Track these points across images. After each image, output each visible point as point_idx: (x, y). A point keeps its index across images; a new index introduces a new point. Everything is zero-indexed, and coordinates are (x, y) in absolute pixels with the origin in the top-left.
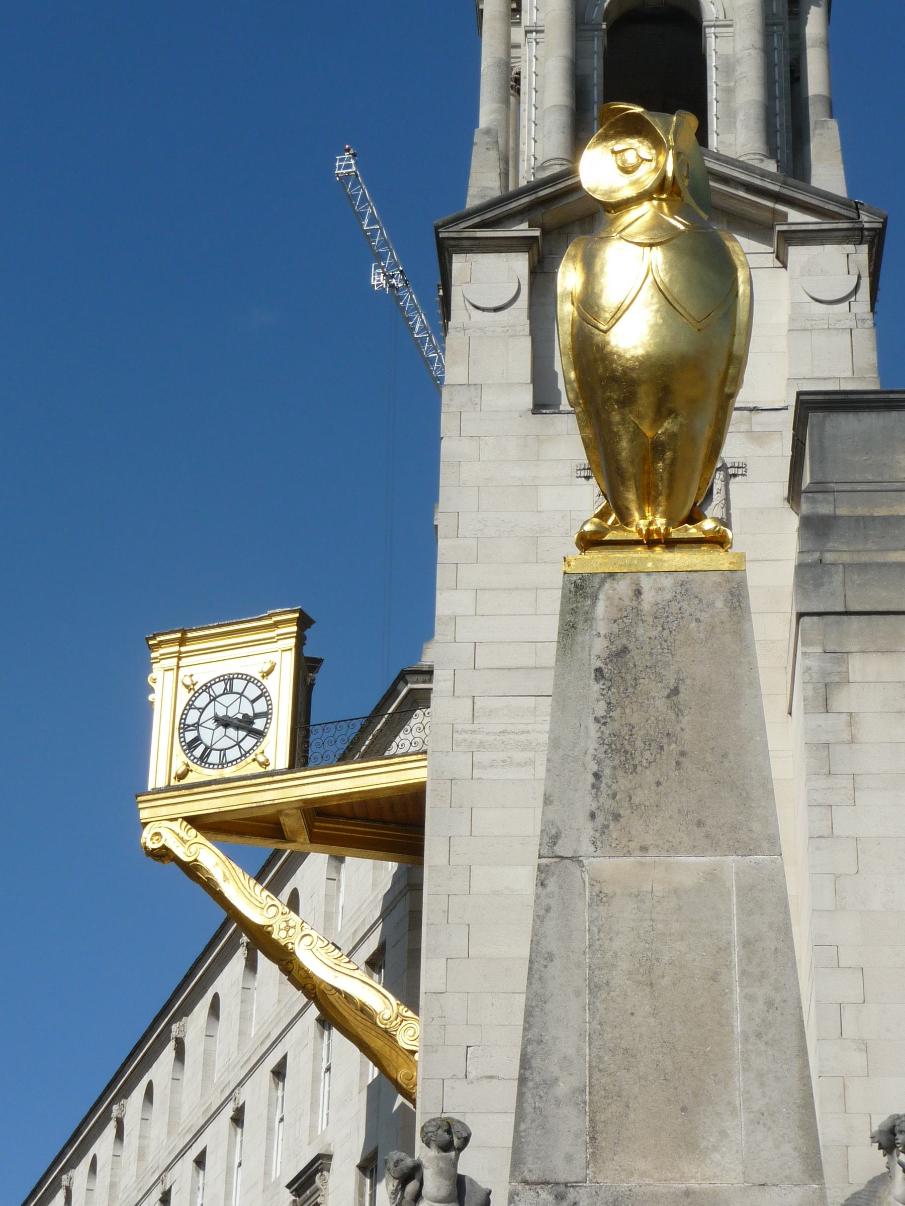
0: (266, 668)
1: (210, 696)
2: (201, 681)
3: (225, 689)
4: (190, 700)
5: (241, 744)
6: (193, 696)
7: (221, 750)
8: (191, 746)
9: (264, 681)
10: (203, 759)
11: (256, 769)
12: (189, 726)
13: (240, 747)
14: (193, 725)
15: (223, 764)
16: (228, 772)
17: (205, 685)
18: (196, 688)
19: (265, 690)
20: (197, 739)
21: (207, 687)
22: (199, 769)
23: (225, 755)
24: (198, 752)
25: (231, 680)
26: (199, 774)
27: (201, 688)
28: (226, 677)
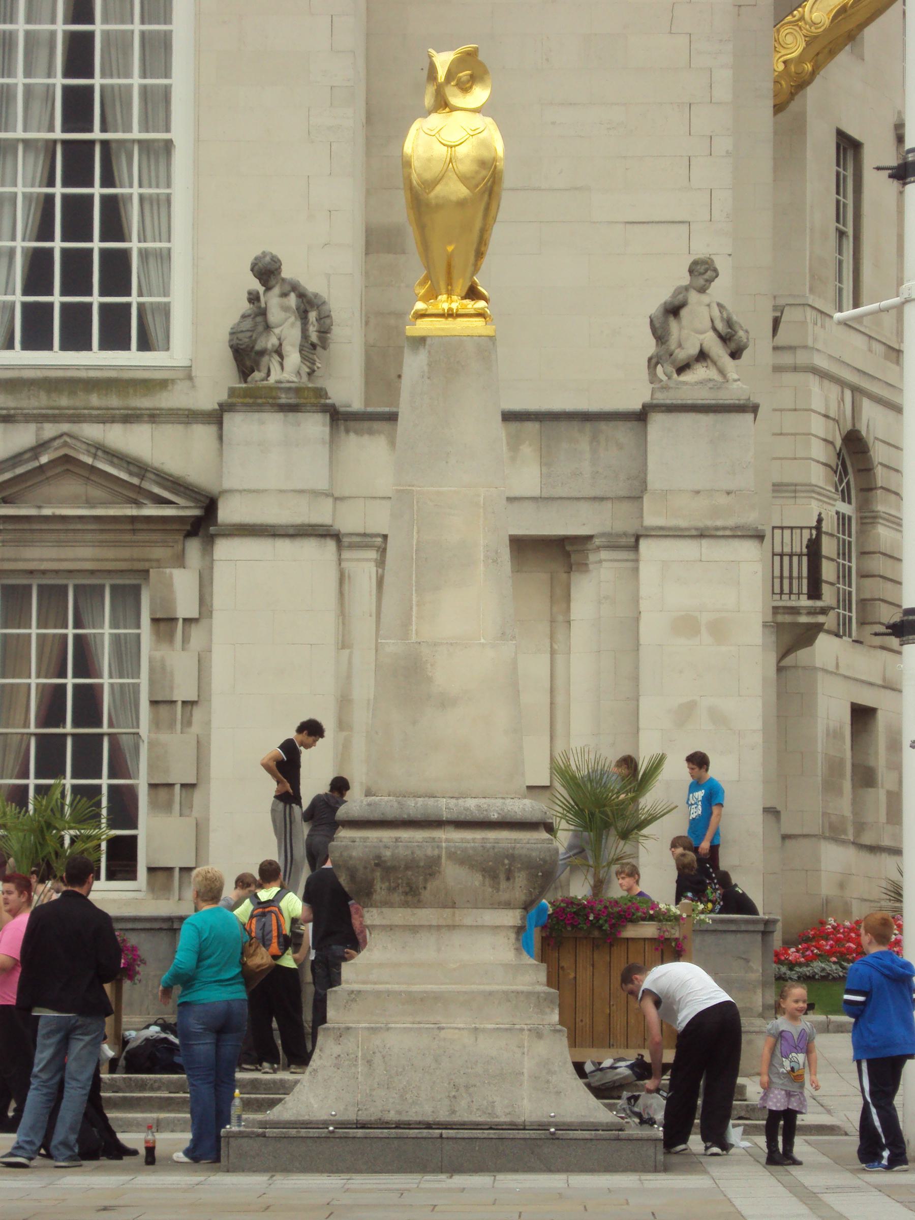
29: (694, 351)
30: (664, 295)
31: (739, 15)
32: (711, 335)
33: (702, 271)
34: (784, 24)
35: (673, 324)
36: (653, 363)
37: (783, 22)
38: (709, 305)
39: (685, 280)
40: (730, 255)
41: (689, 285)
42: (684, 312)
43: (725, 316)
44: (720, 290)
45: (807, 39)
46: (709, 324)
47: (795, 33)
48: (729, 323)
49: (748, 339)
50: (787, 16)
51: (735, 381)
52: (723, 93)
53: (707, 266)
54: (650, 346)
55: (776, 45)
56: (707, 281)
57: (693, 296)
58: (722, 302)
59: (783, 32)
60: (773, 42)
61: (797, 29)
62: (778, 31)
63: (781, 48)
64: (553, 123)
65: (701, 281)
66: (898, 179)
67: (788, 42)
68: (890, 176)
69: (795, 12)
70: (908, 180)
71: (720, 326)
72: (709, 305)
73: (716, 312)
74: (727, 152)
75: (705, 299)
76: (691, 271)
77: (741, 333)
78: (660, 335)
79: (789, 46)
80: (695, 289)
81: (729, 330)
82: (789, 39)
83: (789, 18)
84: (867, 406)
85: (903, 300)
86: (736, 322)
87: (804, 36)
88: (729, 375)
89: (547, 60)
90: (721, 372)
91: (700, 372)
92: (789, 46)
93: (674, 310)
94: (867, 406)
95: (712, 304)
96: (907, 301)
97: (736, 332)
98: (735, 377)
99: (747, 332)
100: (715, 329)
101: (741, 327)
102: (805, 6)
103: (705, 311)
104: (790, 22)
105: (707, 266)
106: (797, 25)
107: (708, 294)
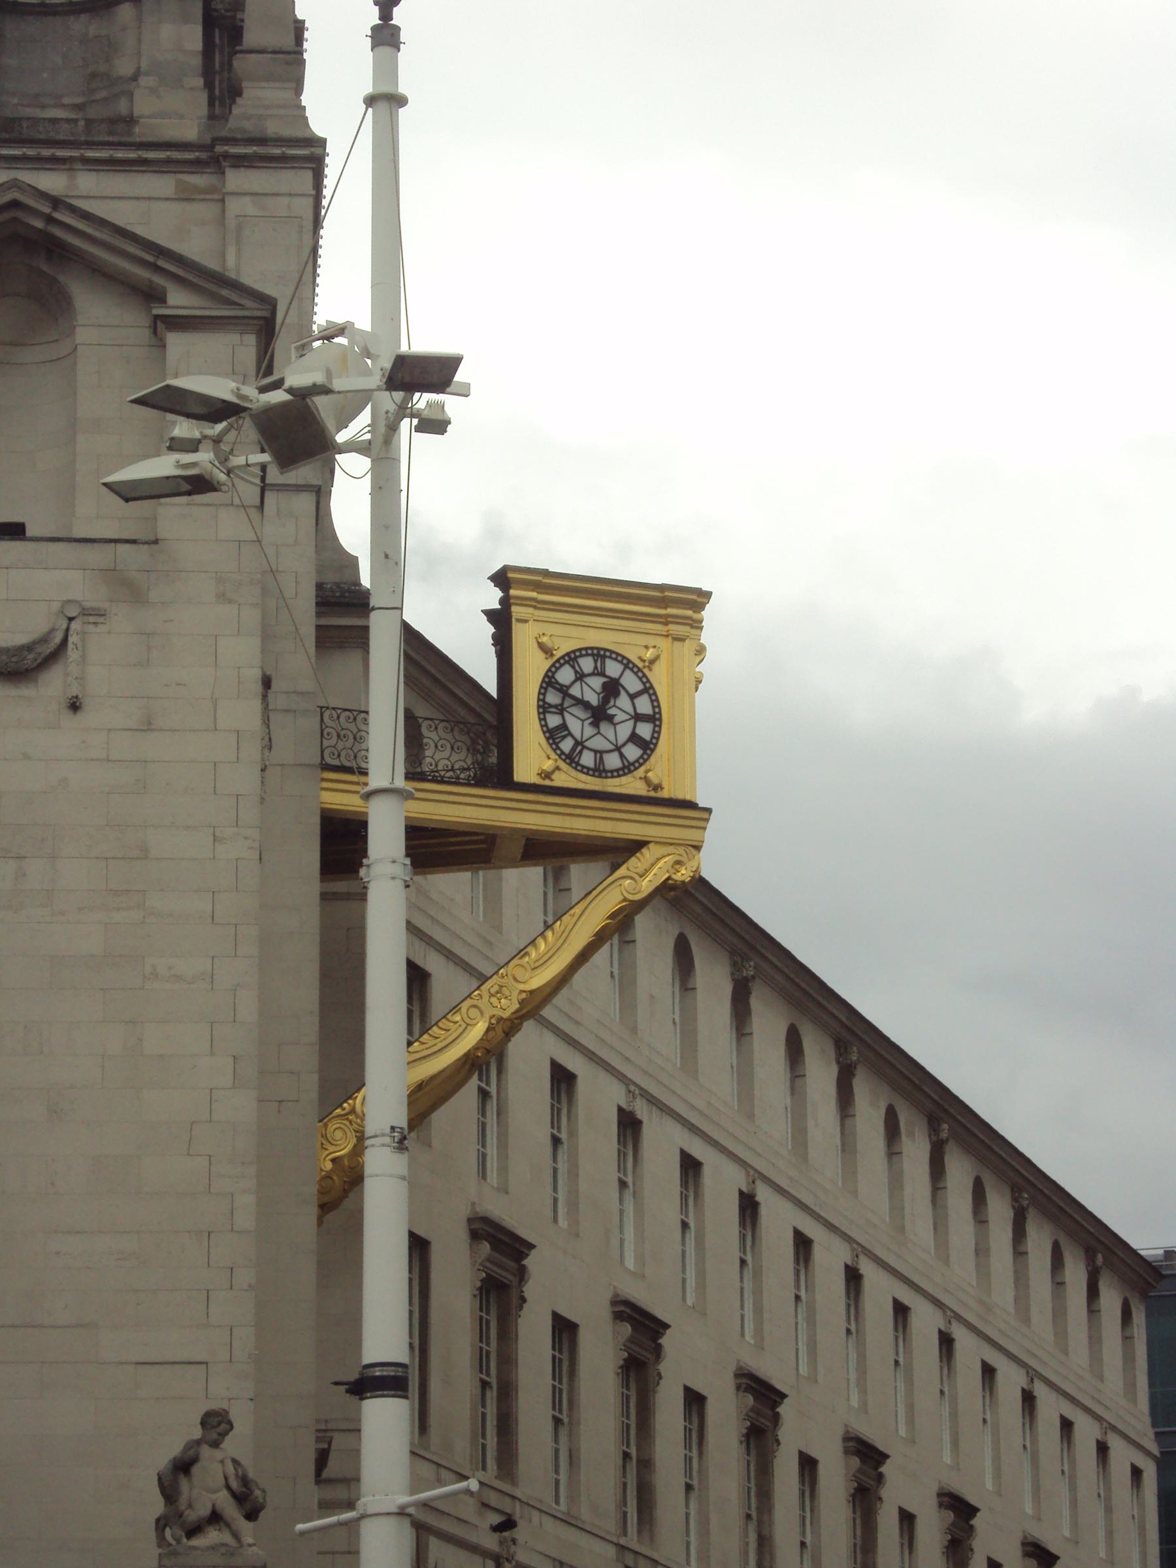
0: (649, 654)
1: (576, 672)
2: (563, 648)
3: (596, 668)
4: (549, 670)
5: (624, 750)
6: (553, 665)
7: (596, 752)
8: (553, 736)
9: (646, 671)
10: (571, 759)
11: (639, 788)
12: (551, 706)
13: (622, 756)
14: (555, 706)
15: (599, 771)
16: (613, 785)
17: (568, 654)
18: (558, 654)
19: (648, 685)
20: (564, 726)
21: (571, 658)
22: (573, 773)
23: (601, 759)
24: (567, 745)
25: (604, 657)
26: (566, 778)
27: (563, 657)
28: (595, 652)
29: (203, 1510)
30: (173, 1448)
31: (279, 1111)
32: (224, 1494)
33: (215, 1424)
34: (332, 1118)
35: (184, 1483)
36: (161, 1524)
37: (331, 1116)
38: (222, 1462)
39: (197, 1433)
40: (251, 1400)
41: (201, 1439)
42: (195, 1470)
43: (240, 1473)
44: (232, 1446)
45: (358, 1134)
46: (222, 1481)
47: (345, 1128)
48: (245, 1480)
49: (264, 1499)
50: (336, 1109)
51: (250, 1545)
52: (245, 1220)
53: (220, 1418)
54: (157, 1506)
55: (324, 1142)
56: (220, 1434)
57: (206, 1451)
58: (237, 1458)
59: (332, 1126)
60: (320, 1138)
61: (347, 1123)
62: (326, 1125)
63: (328, 1144)
64: (58, 1253)
65: (214, 1435)
66: (355, 1395)
67: (337, 1139)
68: (347, 1391)
69: (345, 1105)
70: (364, 1395)
71: (234, 1484)
72: (222, 1462)
73: (230, 1469)
74: (250, 1285)
75: (218, 1454)
76: (203, 1424)
77: (257, 1492)
78: (169, 1492)
79: (339, 1142)
80: (206, 1443)
81: (244, 1489)
82: (339, 1134)
83: (338, 1111)
84: (434, 1544)
85: (359, 1516)
86: (251, 1480)
87: (355, 1131)
88: (243, 1539)
89: (52, 1184)
90: (236, 1536)
91: (213, 1536)
92: (339, 1142)
93: (184, 1466)
94: (434, 1544)
95: (226, 1460)
96: (363, 1516)
97: (252, 1492)
98: (251, 1541)
99: (264, 1491)
100: (228, 1488)
101: (257, 1485)
102: (356, 1097)
103: (217, 1467)
104: (339, 1116)
105: (220, 1418)
106: (347, 1119)
107: (222, 1449)
